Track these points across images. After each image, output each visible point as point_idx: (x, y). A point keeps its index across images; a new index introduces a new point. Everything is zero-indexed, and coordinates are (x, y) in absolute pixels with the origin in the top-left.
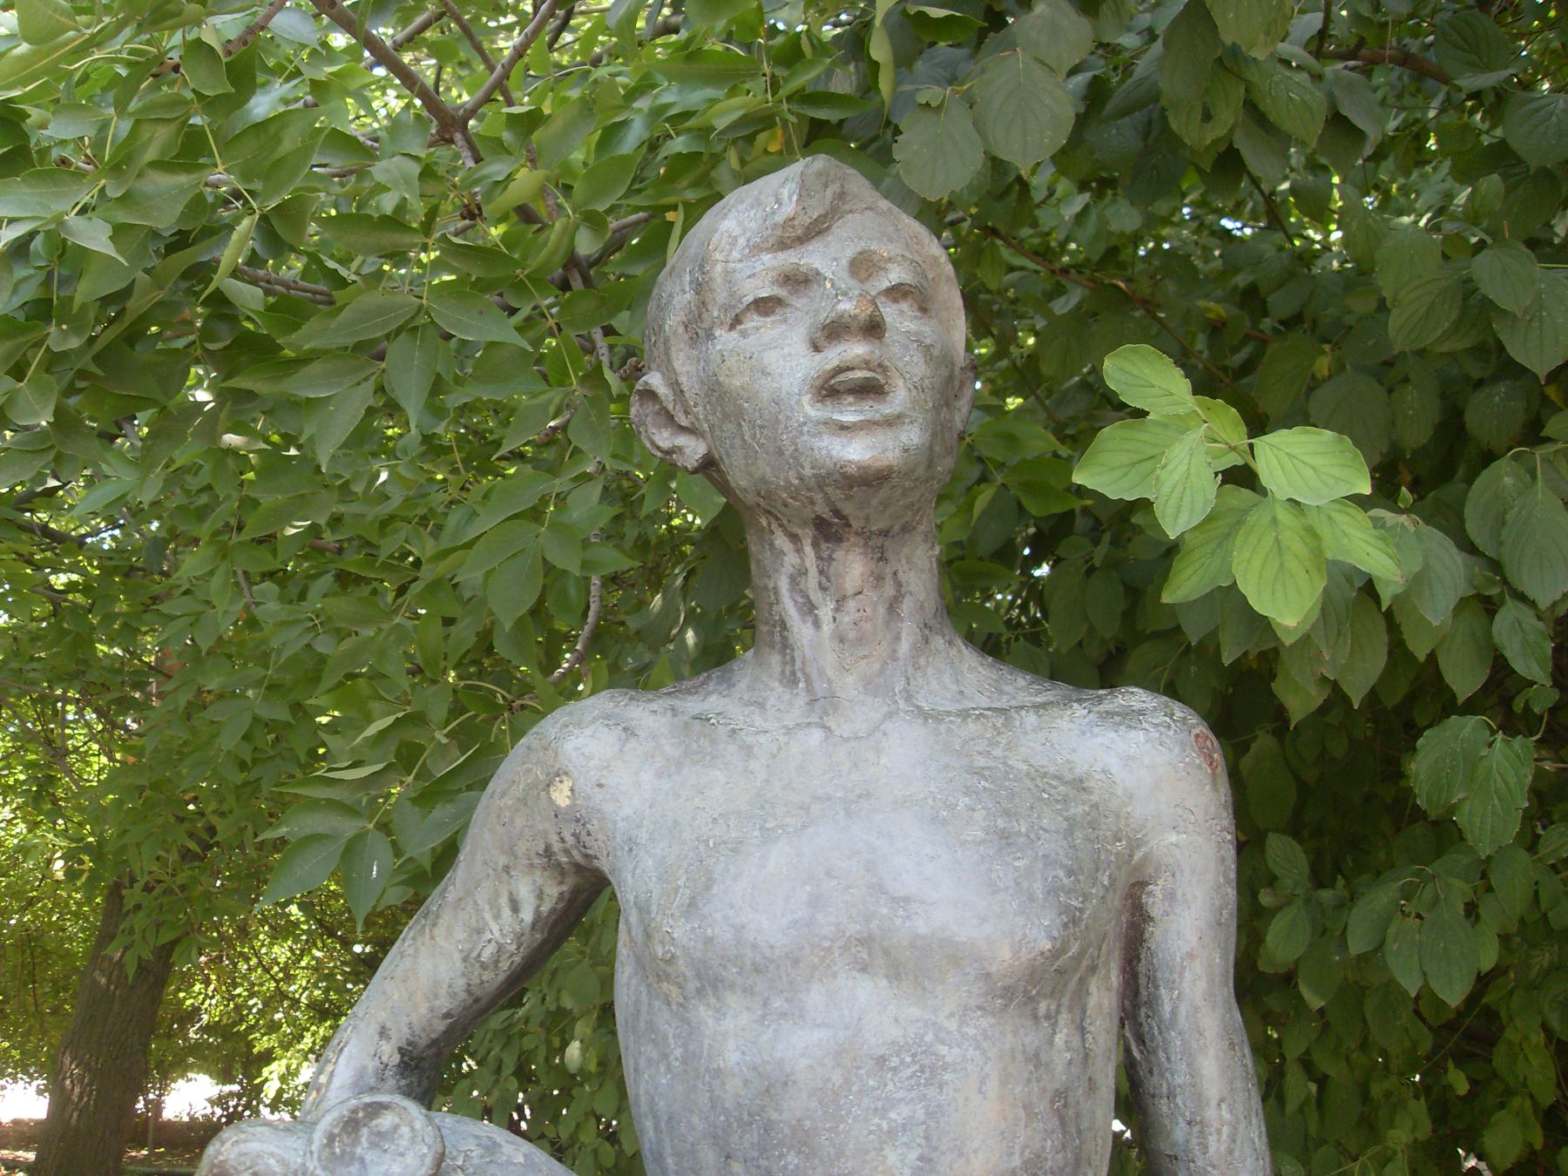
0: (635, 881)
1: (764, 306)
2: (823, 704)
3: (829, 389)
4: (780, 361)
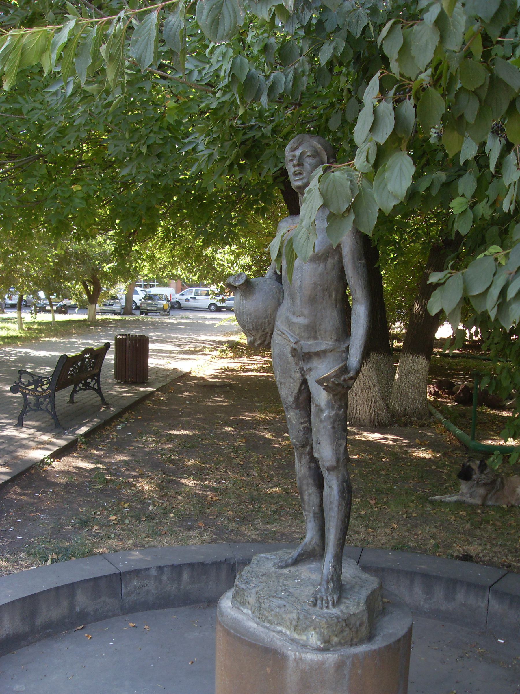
1: (291, 160)
3: (295, 174)
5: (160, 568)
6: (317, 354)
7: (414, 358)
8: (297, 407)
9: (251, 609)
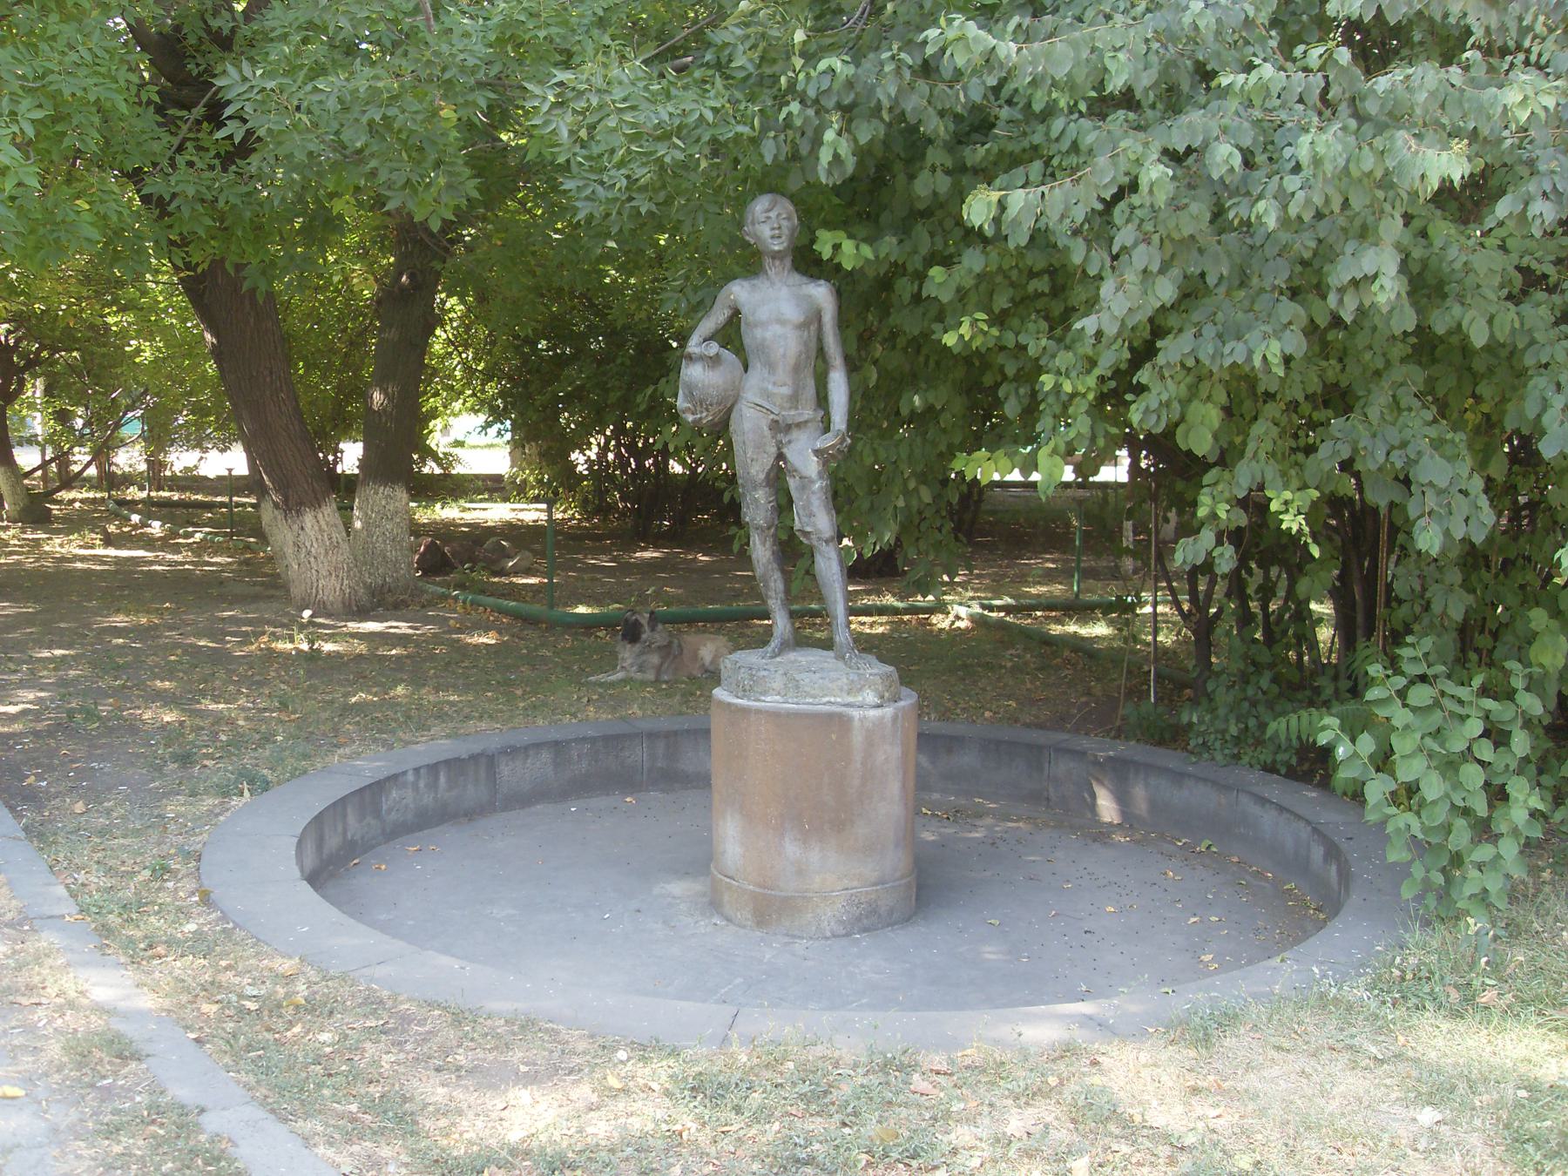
0: (745, 310)
2: (773, 284)
4: (765, 231)
5: (417, 770)
6: (799, 425)
7: (388, 491)
8: (768, 485)
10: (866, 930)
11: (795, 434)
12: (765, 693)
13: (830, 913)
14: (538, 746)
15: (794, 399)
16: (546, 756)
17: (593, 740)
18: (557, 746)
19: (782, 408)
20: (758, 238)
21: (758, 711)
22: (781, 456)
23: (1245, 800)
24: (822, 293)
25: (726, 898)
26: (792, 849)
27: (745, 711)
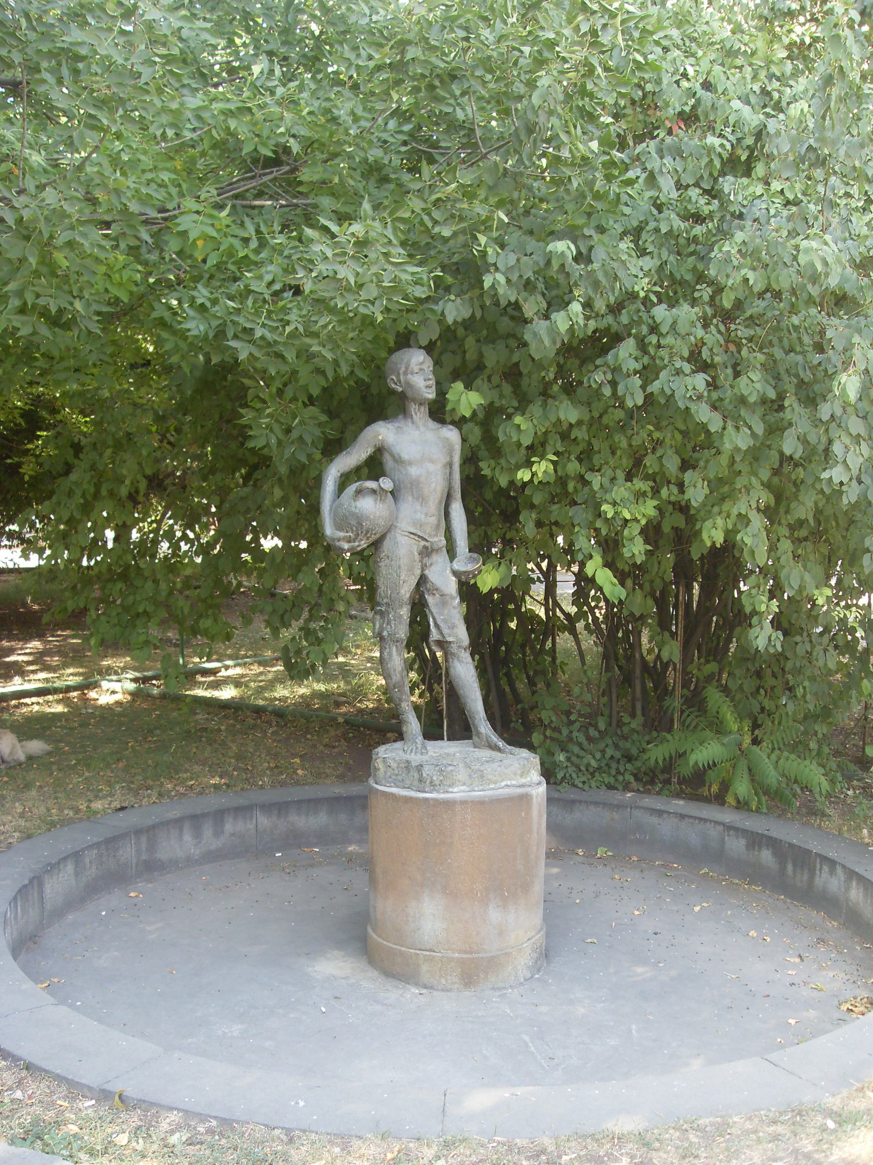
2: (418, 428)
9: (464, 784)
10: (539, 970)
11: (435, 557)
12: (452, 785)
13: (523, 961)
14: (65, 859)
15: (438, 526)
16: (70, 867)
17: (97, 845)
18: (76, 856)
19: (430, 536)
20: (409, 384)
21: (464, 802)
22: (423, 580)
23: (636, 813)
24: (452, 435)
25: (424, 968)
26: (494, 915)
27: (448, 804)
